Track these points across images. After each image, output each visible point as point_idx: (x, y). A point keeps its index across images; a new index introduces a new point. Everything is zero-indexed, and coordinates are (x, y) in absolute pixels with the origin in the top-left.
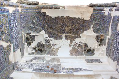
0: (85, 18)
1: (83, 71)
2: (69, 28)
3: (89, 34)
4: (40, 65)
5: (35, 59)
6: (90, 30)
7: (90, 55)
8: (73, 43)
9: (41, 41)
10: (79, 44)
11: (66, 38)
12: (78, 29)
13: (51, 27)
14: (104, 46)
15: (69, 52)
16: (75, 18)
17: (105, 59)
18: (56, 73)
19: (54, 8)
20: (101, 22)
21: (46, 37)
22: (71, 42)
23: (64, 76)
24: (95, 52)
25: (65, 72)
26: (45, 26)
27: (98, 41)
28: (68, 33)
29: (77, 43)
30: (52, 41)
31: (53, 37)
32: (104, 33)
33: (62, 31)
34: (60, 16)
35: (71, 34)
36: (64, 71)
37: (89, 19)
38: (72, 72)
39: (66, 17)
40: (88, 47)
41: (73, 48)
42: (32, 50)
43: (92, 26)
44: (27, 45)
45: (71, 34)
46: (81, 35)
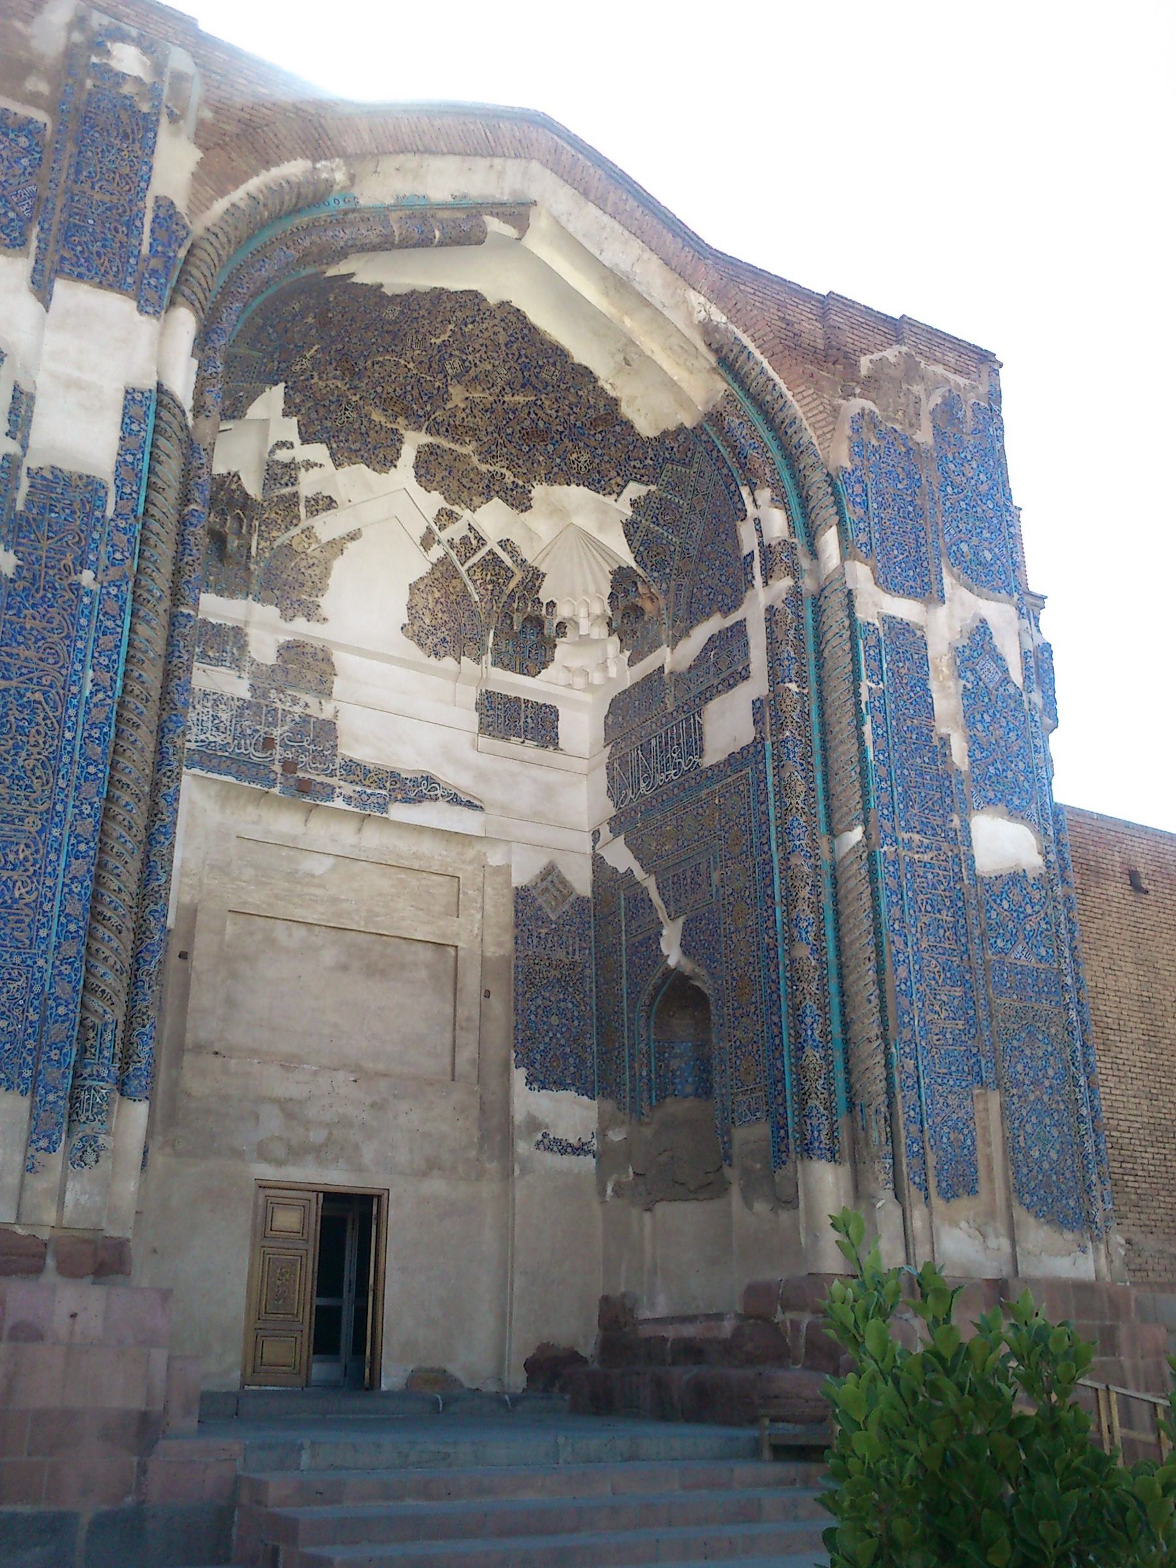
0: (631, 400)
1: (442, 804)
3: (585, 521)
4: (224, 717)
6: (610, 500)
8: (456, 531)
9: (234, 469)
10: (491, 552)
11: (429, 468)
12: (535, 435)
14: (628, 653)
15: (406, 598)
16: (559, 353)
17: (582, 727)
18: (307, 800)
19: (441, 244)
20: (699, 528)
21: (281, 445)
22: (446, 517)
24: (562, 650)
25: (348, 800)
26: (300, 350)
28: (453, 430)
30: (320, 471)
32: (672, 595)
33: (417, 403)
34: (455, 285)
35: (467, 450)
36: (348, 789)
37: (651, 436)
38: (383, 807)
39: (503, 304)
40: (545, 596)
41: (441, 561)
43: (634, 490)
45: (467, 450)
46: (539, 491)
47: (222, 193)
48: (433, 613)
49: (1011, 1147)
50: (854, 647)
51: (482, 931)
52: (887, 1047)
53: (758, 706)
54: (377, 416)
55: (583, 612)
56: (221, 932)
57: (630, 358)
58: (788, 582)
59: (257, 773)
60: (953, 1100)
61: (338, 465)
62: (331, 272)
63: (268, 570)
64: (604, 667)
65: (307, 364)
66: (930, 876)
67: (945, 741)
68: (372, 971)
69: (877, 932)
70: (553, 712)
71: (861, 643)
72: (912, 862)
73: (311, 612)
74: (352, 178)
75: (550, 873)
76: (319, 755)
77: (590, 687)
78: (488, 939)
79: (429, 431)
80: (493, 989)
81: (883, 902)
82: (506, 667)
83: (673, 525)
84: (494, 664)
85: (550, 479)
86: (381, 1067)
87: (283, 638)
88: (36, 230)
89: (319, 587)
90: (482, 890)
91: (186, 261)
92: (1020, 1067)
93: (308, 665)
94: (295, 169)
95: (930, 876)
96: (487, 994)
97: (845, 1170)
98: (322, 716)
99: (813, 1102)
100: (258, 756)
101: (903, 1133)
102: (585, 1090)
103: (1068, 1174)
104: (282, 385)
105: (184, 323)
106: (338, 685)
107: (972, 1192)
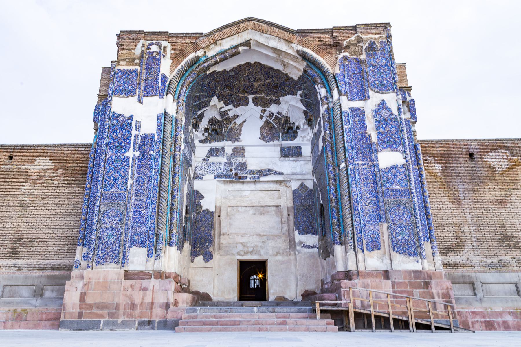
1: (272, 175)
2: (260, 83)
3: (293, 103)
5: (212, 152)
6: (295, 96)
7: (290, 140)
11: (256, 102)
12: (276, 87)
13: (228, 87)
15: (259, 131)
16: (271, 68)
17: (307, 150)
18: (241, 180)
19: (230, 57)
21: (221, 108)
22: (263, 111)
23: (248, 182)
24: (299, 132)
25: (250, 178)
26: (216, 88)
27: (305, 118)
29: (272, 113)
30: (232, 111)
31: (232, 104)
33: (248, 89)
34: (242, 63)
35: (263, 95)
36: (250, 176)
38: (258, 178)
40: (291, 122)
41: (266, 121)
42: (203, 134)
43: (299, 92)
44: (195, 131)
45: (263, 95)
46: (281, 99)
47: (177, 67)
48: (266, 133)
49: (391, 237)
50: (341, 118)
51: (286, 200)
52: (352, 216)
53: (324, 137)
54: (241, 95)
55: (301, 123)
56: (227, 210)
57: (285, 65)
58: (326, 106)
59: (230, 176)
60: (372, 227)
61: (236, 108)
62: (208, 72)
63: (228, 133)
64: (308, 134)
65: (219, 90)
66: (365, 171)
67: (370, 136)
68: (261, 214)
69: (349, 188)
70: (300, 148)
71: (343, 117)
72: (359, 169)
73: (238, 140)
74: (205, 52)
75: (302, 185)
76: (242, 171)
77: (308, 140)
78: (288, 203)
79: (253, 94)
80: (290, 213)
81: (350, 180)
82: (285, 140)
83: (309, 98)
84: (282, 140)
85: (283, 96)
86: (265, 234)
87: (233, 147)
88: (138, 90)
89: (239, 134)
90: (286, 192)
91: (169, 84)
92: (394, 216)
93: (239, 151)
94: (192, 56)
95: (365, 171)
96: (289, 215)
97: (343, 247)
98: (243, 162)
99: (335, 231)
100: (229, 173)
101: (356, 236)
102: (313, 234)
103: (412, 242)
104: (215, 96)
105: (170, 97)
106: (246, 154)
107: (379, 249)
